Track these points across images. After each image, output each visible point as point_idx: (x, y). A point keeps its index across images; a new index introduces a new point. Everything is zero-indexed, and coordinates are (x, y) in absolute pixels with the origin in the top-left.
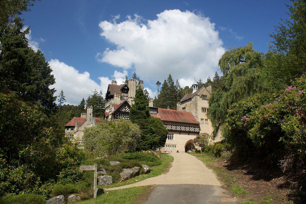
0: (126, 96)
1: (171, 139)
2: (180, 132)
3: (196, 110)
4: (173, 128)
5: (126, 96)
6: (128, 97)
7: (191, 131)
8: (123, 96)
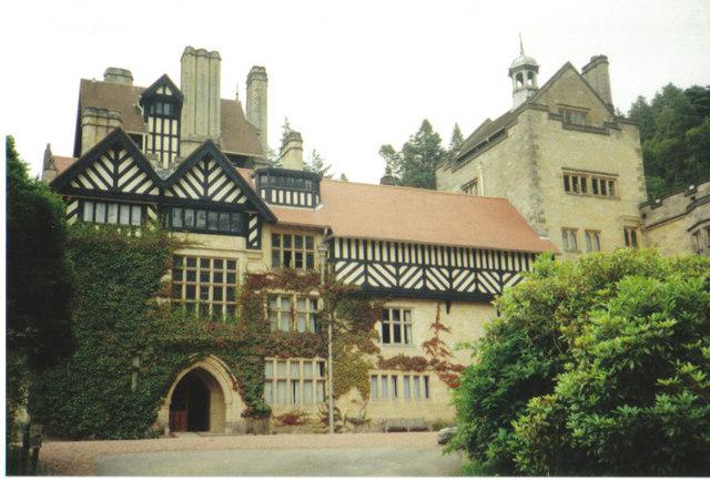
0: (170, 136)
1: (397, 339)
3: (536, 181)
4: (345, 272)
6: (178, 136)
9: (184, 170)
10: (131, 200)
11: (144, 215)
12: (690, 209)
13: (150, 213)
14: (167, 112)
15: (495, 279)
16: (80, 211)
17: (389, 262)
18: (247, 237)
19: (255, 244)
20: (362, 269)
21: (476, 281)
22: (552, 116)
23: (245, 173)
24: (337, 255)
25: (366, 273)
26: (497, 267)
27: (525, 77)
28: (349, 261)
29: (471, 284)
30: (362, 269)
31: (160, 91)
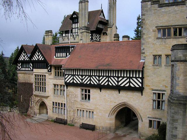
0: (77, 28)
2: (100, 87)
14: (76, 22)
17: (80, 75)
19: (50, 71)
21: (108, 81)
31: (74, 16)
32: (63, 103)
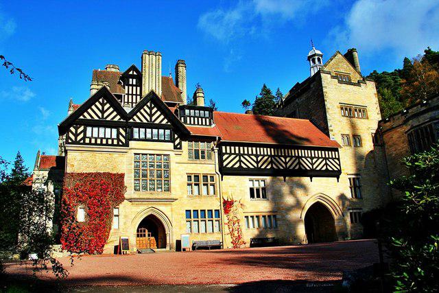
0: (136, 95)
5: (136, 95)
6: (141, 95)
7: (318, 169)
8: (128, 94)
9: (139, 107)
10: (111, 125)
11: (119, 133)
12: (405, 122)
13: (121, 130)
14: (134, 83)
15: (317, 161)
16: (84, 131)
17: (252, 154)
18: (174, 142)
19: (179, 146)
20: (237, 158)
22: (333, 77)
23: (173, 109)
24: (224, 151)
25: (240, 161)
26: (310, 156)
27: (316, 60)
28: (231, 154)
29: (315, 162)
30: (237, 158)
31: (131, 73)
32: (214, 208)
